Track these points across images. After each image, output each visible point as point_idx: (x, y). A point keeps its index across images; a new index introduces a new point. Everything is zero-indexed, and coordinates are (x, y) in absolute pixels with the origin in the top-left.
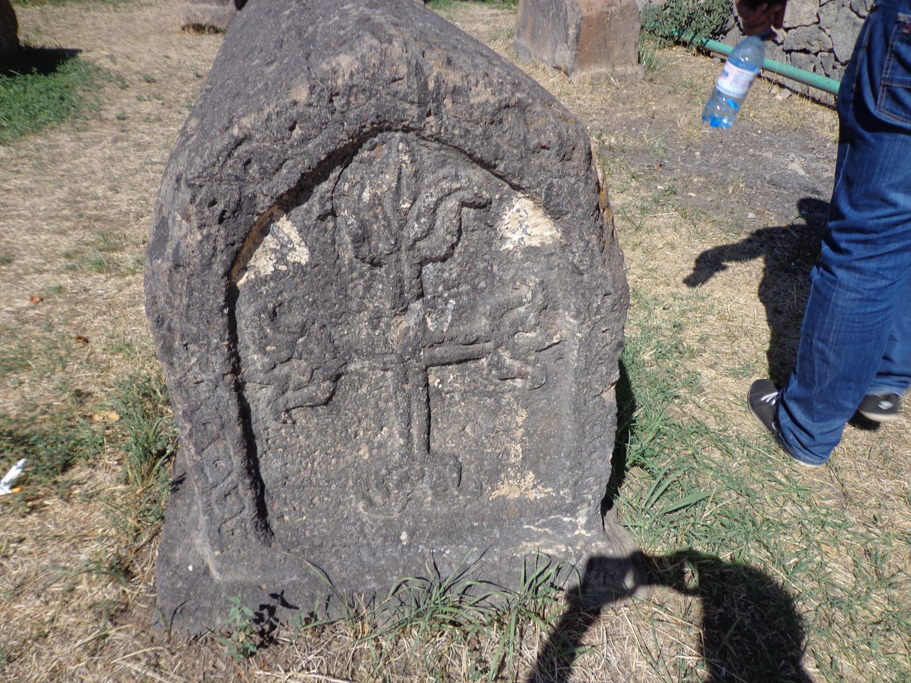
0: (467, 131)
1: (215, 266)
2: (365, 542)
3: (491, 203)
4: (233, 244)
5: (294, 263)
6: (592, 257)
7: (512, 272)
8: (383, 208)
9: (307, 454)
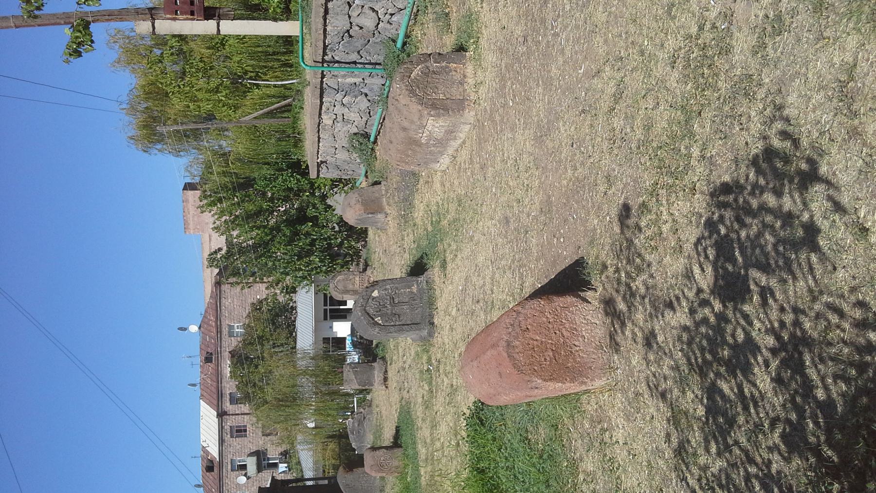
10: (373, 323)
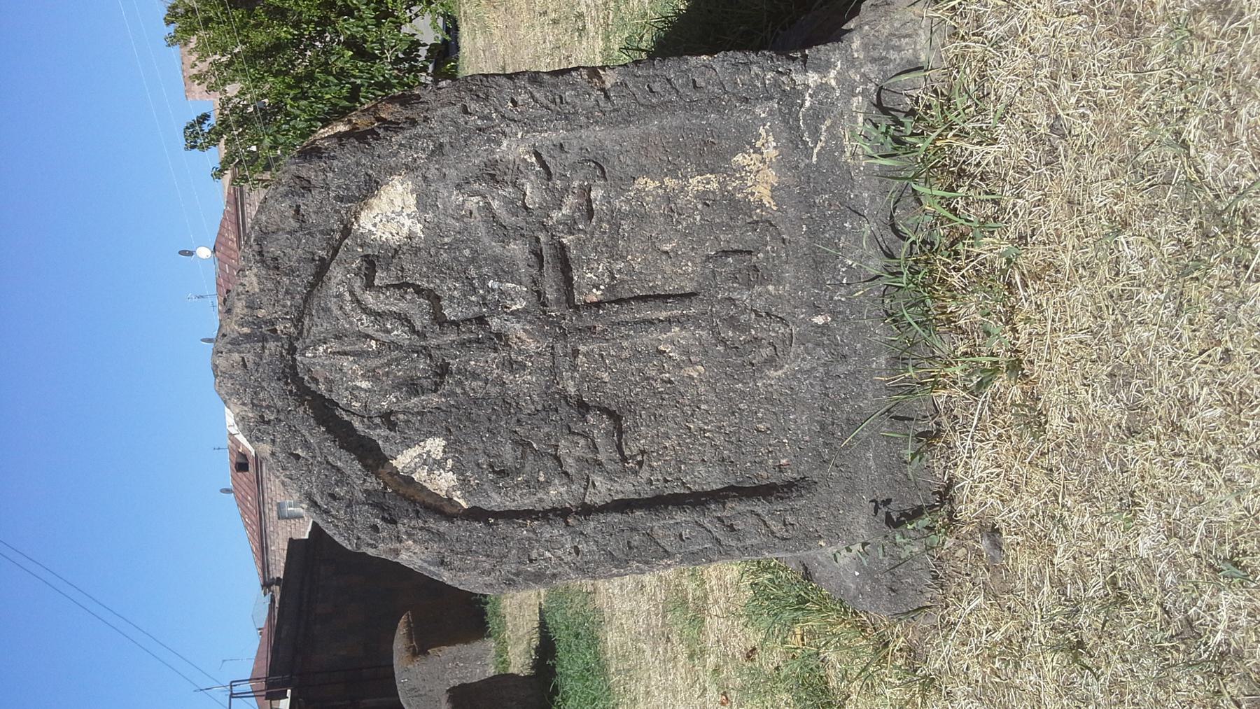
0: (287, 292)
1: (442, 529)
2: (821, 369)
3: (367, 256)
4: (417, 512)
5: (444, 452)
6: (418, 137)
7: (450, 221)
8: (377, 367)
9: (690, 437)
10: (376, 502)
